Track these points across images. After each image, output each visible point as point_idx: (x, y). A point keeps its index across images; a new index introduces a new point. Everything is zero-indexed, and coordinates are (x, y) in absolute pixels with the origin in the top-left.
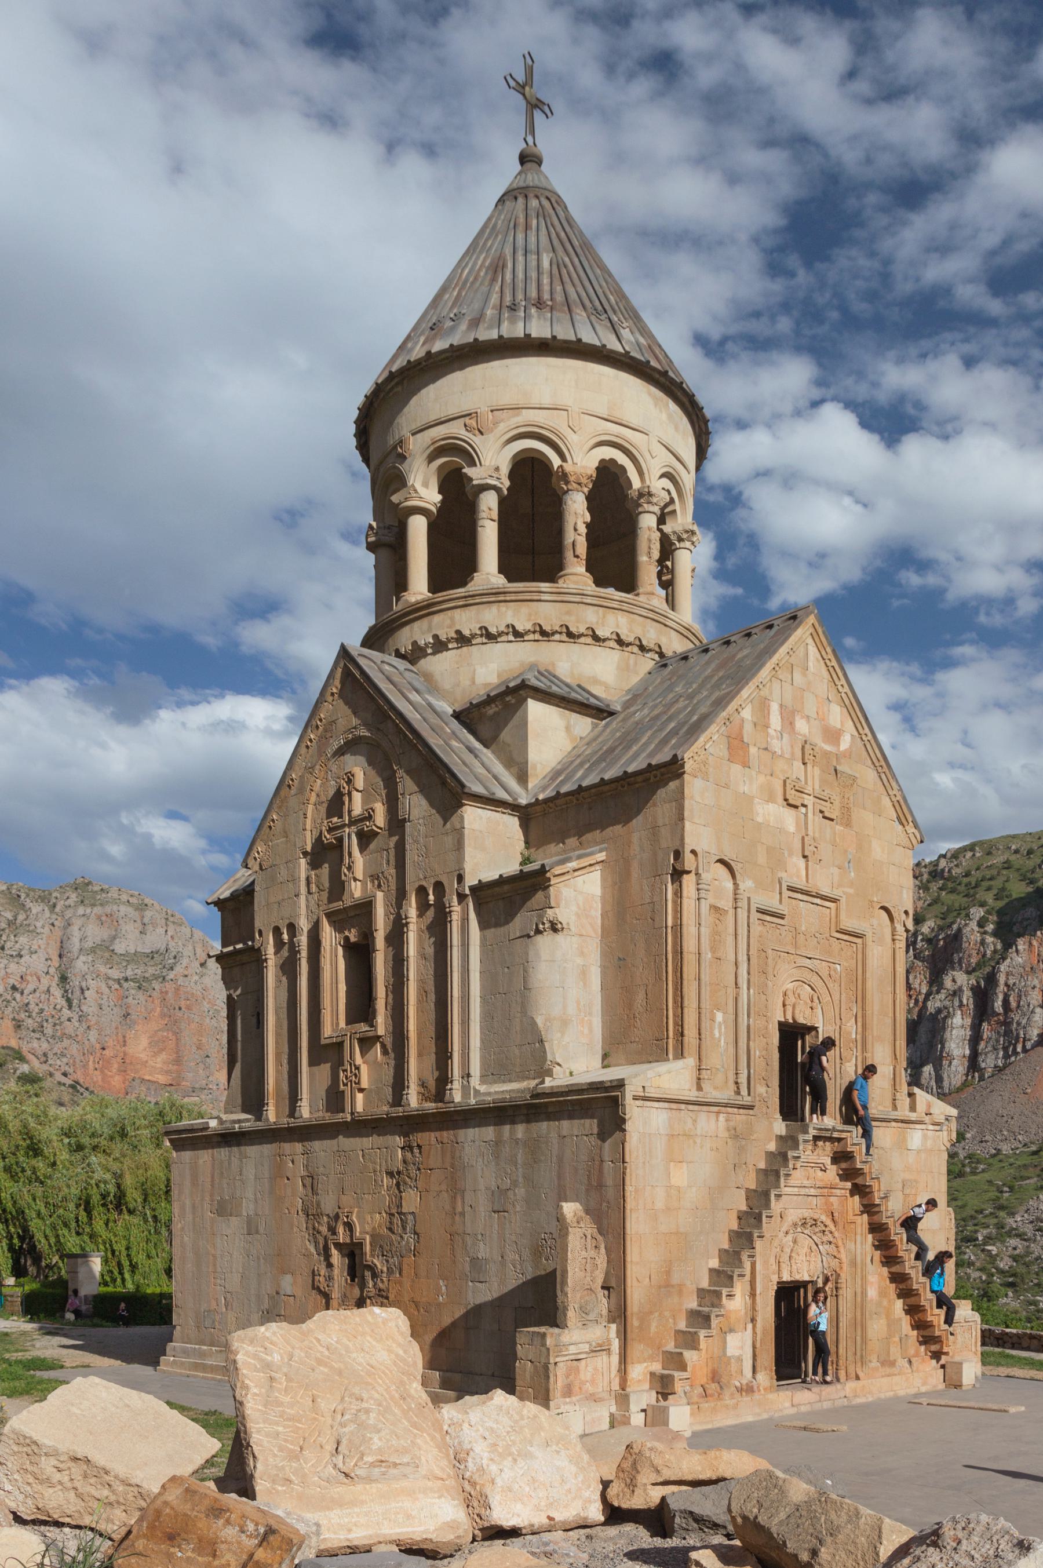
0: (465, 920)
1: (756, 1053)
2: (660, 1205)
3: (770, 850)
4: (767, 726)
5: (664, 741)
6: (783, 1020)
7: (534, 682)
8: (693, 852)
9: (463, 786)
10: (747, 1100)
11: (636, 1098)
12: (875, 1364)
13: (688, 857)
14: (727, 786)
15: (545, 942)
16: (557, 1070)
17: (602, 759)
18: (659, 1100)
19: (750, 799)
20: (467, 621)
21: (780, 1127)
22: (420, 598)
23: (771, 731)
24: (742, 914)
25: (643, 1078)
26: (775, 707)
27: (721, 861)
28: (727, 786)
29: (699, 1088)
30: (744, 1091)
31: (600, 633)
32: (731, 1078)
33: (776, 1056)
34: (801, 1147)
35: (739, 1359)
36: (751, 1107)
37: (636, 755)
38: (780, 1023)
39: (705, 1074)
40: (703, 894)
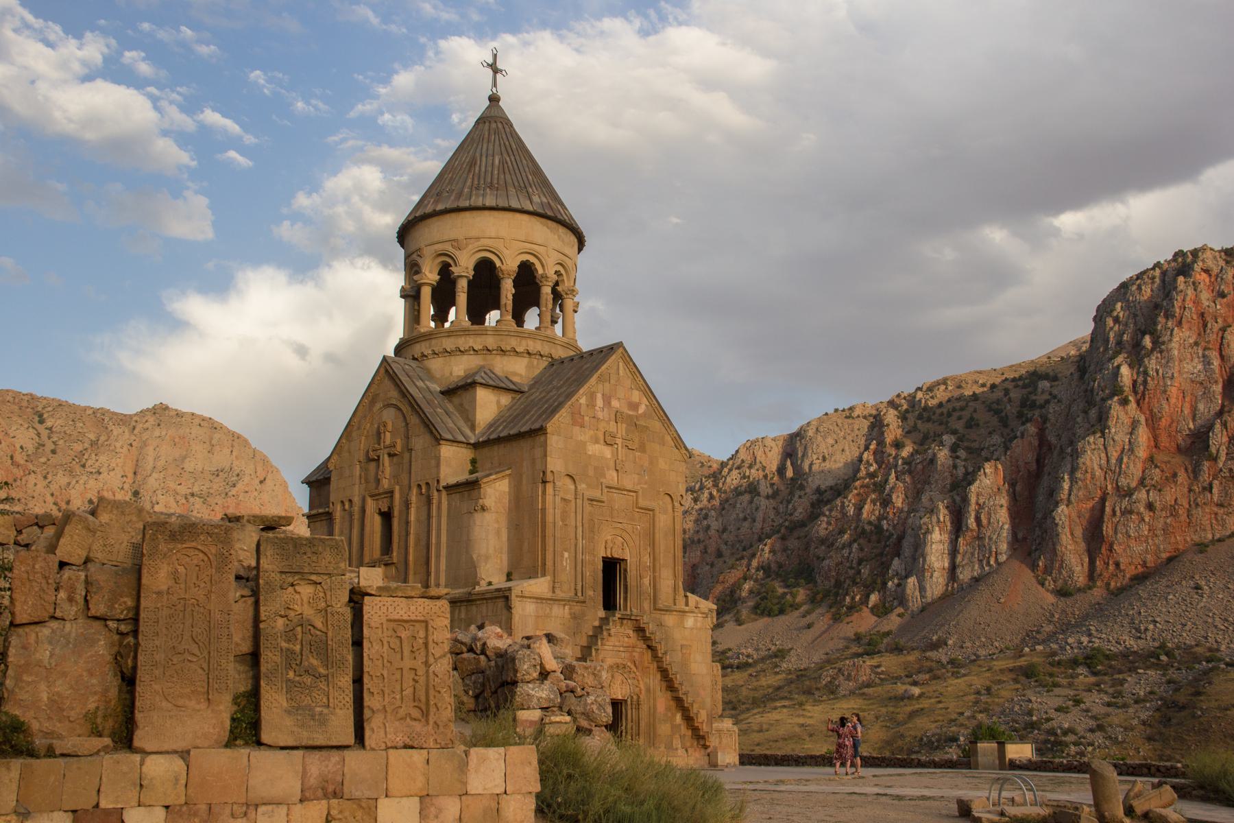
0: (440, 502)
3: (596, 468)
5: (540, 416)
10: (581, 598)
13: (548, 473)
15: (478, 517)
17: (512, 421)
19: (584, 444)
20: (449, 344)
21: (602, 613)
24: (579, 502)
26: (599, 396)
33: (600, 575)
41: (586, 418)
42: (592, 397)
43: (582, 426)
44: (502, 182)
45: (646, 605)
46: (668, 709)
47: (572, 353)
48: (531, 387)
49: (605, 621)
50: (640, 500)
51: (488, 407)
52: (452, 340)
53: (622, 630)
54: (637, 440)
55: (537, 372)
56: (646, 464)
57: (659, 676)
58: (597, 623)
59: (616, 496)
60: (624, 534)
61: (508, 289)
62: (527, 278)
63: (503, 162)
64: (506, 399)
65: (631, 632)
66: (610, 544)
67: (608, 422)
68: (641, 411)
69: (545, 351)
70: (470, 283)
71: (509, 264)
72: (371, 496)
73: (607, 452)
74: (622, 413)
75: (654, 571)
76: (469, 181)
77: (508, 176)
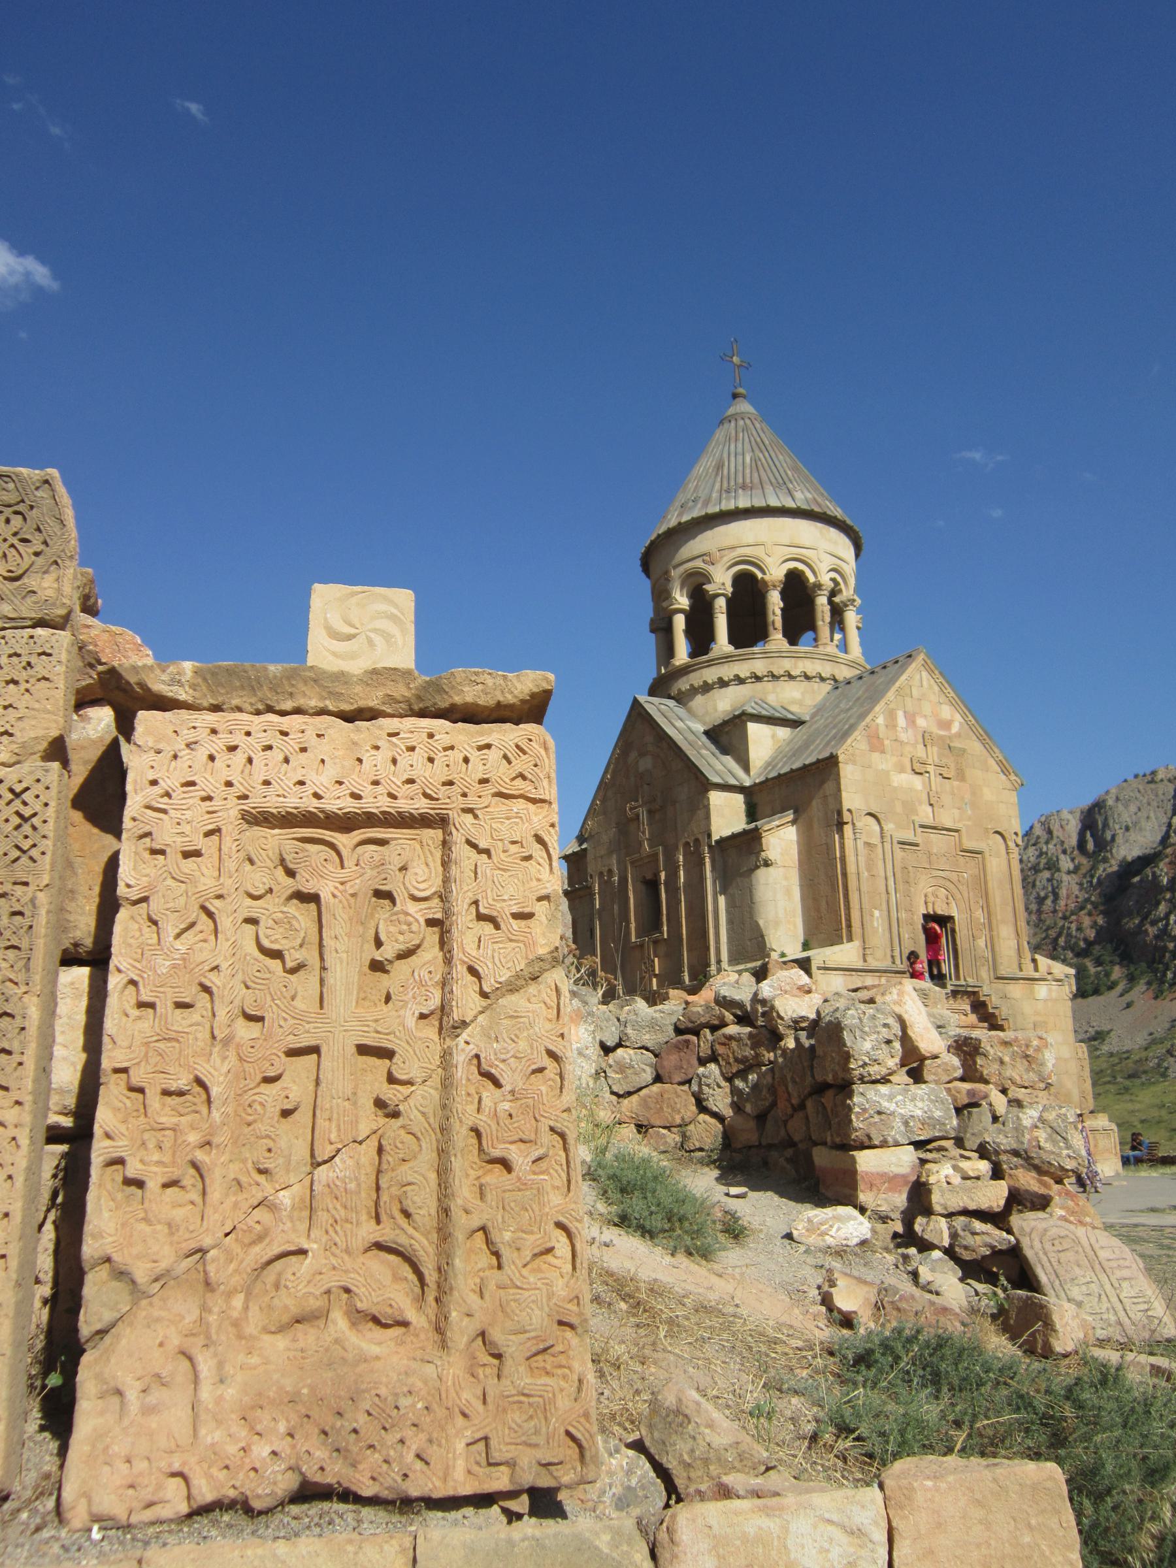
1: (906, 936)
3: (905, 804)
7: (750, 711)
8: (849, 810)
11: (819, 968)
14: (870, 767)
15: (762, 873)
16: (773, 954)
17: (794, 755)
20: (710, 675)
22: (682, 662)
23: (899, 729)
24: (888, 846)
28: (870, 767)
29: (865, 961)
31: (793, 673)
32: (889, 953)
37: (810, 755)
40: (858, 836)
41: (887, 742)
42: (891, 715)
44: (756, 480)
45: (984, 974)
48: (813, 716)
53: (956, 1006)
54: (952, 766)
56: (968, 797)
59: (934, 837)
61: (775, 601)
62: (797, 588)
63: (755, 460)
64: (783, 733)
66: (931, 899)
67: (914, 745)
68: (955, 728)
69: (826, 670)
70: (730, 602)
71: (776, 572)
73: (917, 782)
74: (931, 734)
75: (991, 930)
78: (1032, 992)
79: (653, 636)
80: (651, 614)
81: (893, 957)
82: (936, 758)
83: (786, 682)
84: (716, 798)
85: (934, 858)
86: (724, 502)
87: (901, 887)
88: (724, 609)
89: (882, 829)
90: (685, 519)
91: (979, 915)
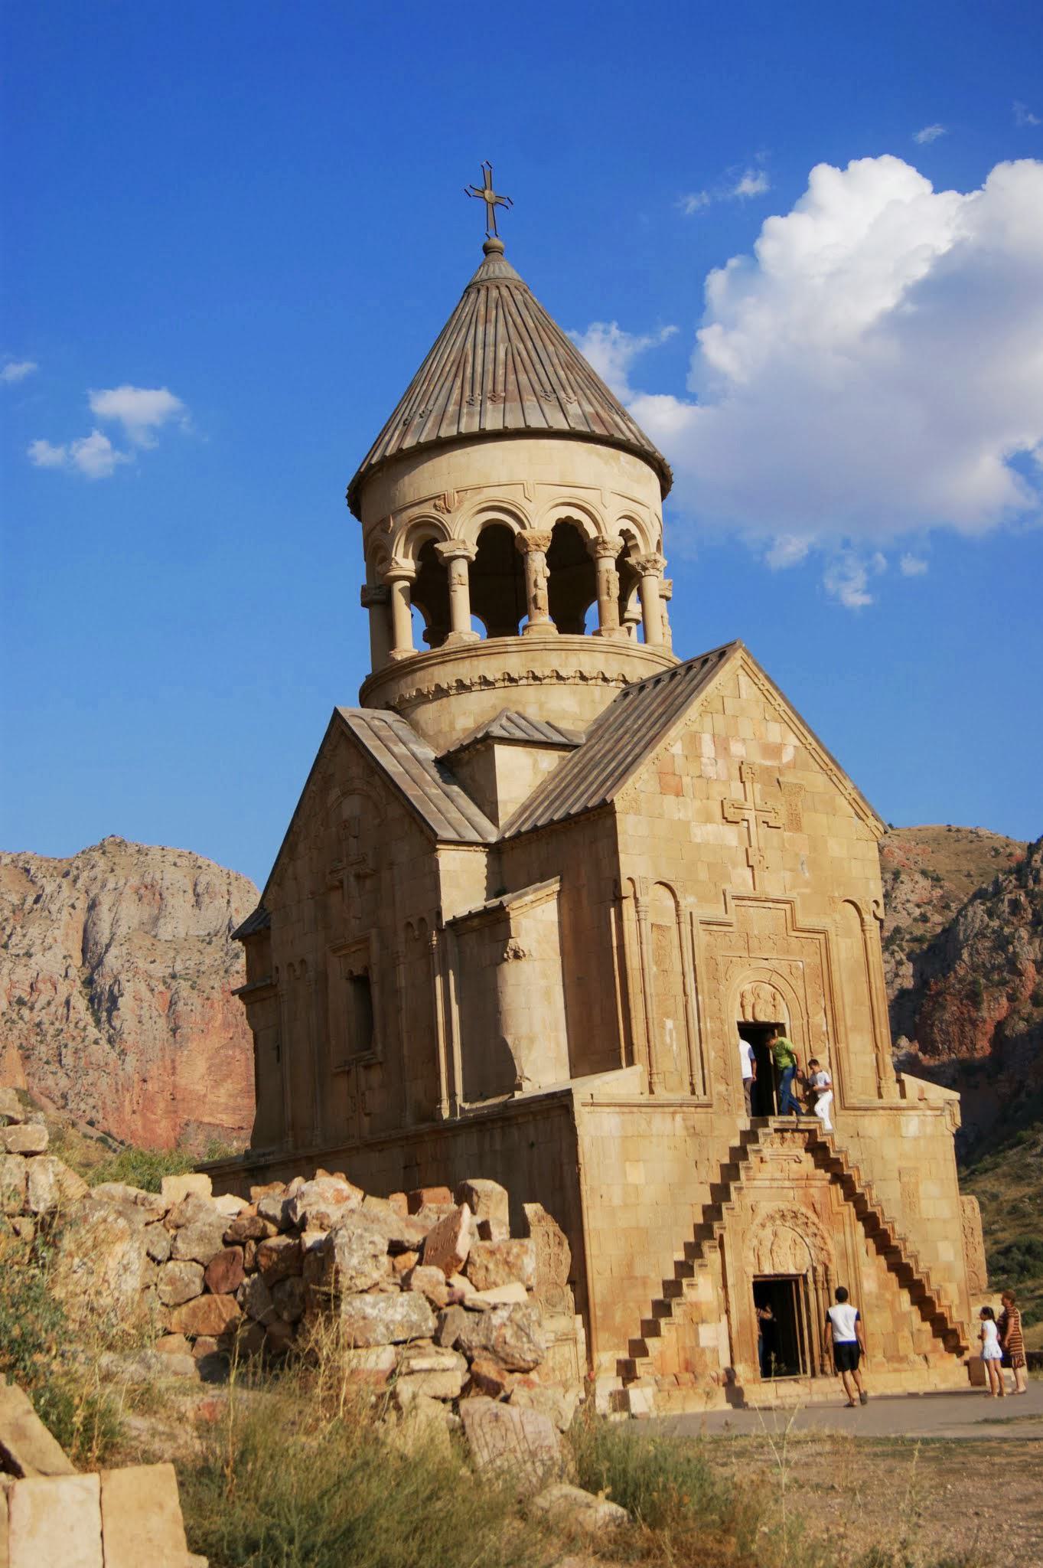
2: (617, 1201)
3: (710, 866)
4: (699, 757)
6: (742, 1020)
9: (436, 835)
10: (703, 1099)
12: (880, 1357)
14: (660, 816)
16: (526, 1085)
18: (608, 1105)
23: (704, 760)
24: (686, 928)
25: (585, 1089)
27: (661, 883)
28: (660, 816)
29: (652, 1092)
30: (699, 1090)
31: (563, 674)
32: (687, 1079)
34: (761, 1140)
35: (715, 1351)
36: (709, 1106)
38: (739, 1024)
39: (655, 1079)
40: (642, 915)
42: (693, 741)
43: (679, 793)
44: (512, 387)
46: (883, 1286)
47: (661, 669)
49: (749, 1136)
50: (799, 917)
51: (520, 777)
52: (449, 666)
53: (784, 1150)
54: (783, 811)
55: (602, 709)
56: (805, 853)
57: (860, 1228)
58: (736, 1142)
60: (777, 980)
61: (539, 568)
62: (571, 545)
64: (549, 761)
65: (802, 1153)
68: (788, 755)
70: (472, 566)
72: (334, 951)
73: (731, 836)
76: (456, 392)
77: (523, 378)
78: (897, 1127)
79: (366, 611)
80: (363, 580)
81: (691, 1084)
82: (758, 801)
83: (559, 681)
84: (448, 860)
85: (754, 943)
86: (464, 420)
87: (705, 984)
88: (466, 579)
89: (677, 903)
90: (409, 443)
91: (820, 1020)
